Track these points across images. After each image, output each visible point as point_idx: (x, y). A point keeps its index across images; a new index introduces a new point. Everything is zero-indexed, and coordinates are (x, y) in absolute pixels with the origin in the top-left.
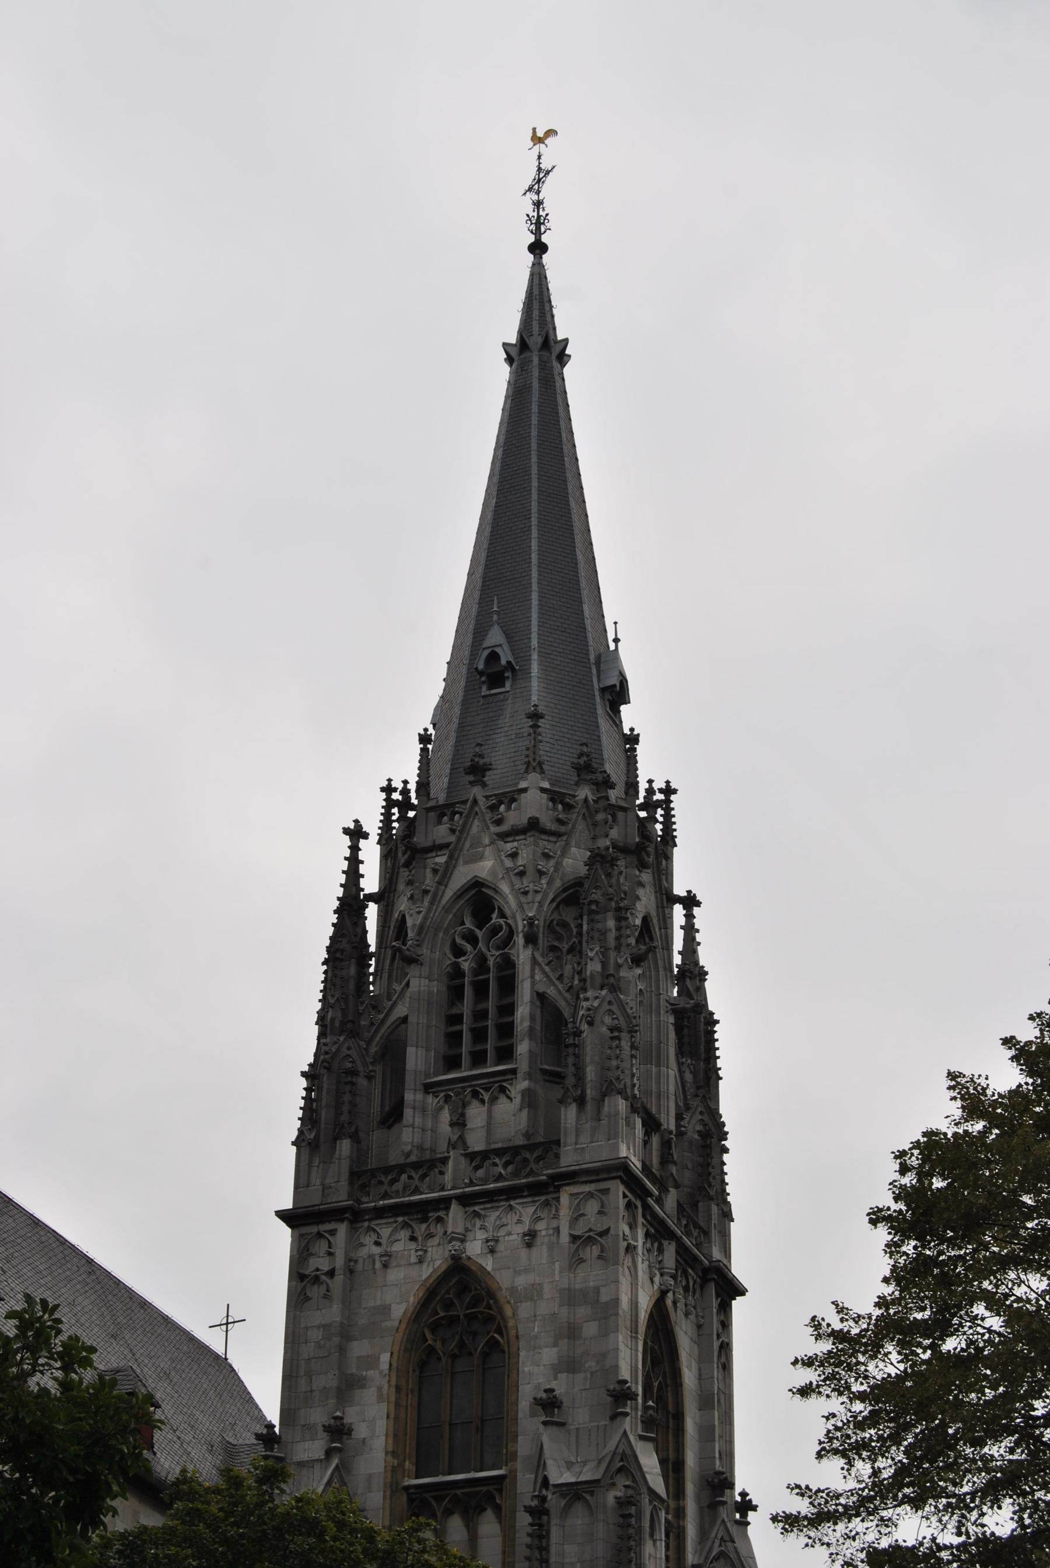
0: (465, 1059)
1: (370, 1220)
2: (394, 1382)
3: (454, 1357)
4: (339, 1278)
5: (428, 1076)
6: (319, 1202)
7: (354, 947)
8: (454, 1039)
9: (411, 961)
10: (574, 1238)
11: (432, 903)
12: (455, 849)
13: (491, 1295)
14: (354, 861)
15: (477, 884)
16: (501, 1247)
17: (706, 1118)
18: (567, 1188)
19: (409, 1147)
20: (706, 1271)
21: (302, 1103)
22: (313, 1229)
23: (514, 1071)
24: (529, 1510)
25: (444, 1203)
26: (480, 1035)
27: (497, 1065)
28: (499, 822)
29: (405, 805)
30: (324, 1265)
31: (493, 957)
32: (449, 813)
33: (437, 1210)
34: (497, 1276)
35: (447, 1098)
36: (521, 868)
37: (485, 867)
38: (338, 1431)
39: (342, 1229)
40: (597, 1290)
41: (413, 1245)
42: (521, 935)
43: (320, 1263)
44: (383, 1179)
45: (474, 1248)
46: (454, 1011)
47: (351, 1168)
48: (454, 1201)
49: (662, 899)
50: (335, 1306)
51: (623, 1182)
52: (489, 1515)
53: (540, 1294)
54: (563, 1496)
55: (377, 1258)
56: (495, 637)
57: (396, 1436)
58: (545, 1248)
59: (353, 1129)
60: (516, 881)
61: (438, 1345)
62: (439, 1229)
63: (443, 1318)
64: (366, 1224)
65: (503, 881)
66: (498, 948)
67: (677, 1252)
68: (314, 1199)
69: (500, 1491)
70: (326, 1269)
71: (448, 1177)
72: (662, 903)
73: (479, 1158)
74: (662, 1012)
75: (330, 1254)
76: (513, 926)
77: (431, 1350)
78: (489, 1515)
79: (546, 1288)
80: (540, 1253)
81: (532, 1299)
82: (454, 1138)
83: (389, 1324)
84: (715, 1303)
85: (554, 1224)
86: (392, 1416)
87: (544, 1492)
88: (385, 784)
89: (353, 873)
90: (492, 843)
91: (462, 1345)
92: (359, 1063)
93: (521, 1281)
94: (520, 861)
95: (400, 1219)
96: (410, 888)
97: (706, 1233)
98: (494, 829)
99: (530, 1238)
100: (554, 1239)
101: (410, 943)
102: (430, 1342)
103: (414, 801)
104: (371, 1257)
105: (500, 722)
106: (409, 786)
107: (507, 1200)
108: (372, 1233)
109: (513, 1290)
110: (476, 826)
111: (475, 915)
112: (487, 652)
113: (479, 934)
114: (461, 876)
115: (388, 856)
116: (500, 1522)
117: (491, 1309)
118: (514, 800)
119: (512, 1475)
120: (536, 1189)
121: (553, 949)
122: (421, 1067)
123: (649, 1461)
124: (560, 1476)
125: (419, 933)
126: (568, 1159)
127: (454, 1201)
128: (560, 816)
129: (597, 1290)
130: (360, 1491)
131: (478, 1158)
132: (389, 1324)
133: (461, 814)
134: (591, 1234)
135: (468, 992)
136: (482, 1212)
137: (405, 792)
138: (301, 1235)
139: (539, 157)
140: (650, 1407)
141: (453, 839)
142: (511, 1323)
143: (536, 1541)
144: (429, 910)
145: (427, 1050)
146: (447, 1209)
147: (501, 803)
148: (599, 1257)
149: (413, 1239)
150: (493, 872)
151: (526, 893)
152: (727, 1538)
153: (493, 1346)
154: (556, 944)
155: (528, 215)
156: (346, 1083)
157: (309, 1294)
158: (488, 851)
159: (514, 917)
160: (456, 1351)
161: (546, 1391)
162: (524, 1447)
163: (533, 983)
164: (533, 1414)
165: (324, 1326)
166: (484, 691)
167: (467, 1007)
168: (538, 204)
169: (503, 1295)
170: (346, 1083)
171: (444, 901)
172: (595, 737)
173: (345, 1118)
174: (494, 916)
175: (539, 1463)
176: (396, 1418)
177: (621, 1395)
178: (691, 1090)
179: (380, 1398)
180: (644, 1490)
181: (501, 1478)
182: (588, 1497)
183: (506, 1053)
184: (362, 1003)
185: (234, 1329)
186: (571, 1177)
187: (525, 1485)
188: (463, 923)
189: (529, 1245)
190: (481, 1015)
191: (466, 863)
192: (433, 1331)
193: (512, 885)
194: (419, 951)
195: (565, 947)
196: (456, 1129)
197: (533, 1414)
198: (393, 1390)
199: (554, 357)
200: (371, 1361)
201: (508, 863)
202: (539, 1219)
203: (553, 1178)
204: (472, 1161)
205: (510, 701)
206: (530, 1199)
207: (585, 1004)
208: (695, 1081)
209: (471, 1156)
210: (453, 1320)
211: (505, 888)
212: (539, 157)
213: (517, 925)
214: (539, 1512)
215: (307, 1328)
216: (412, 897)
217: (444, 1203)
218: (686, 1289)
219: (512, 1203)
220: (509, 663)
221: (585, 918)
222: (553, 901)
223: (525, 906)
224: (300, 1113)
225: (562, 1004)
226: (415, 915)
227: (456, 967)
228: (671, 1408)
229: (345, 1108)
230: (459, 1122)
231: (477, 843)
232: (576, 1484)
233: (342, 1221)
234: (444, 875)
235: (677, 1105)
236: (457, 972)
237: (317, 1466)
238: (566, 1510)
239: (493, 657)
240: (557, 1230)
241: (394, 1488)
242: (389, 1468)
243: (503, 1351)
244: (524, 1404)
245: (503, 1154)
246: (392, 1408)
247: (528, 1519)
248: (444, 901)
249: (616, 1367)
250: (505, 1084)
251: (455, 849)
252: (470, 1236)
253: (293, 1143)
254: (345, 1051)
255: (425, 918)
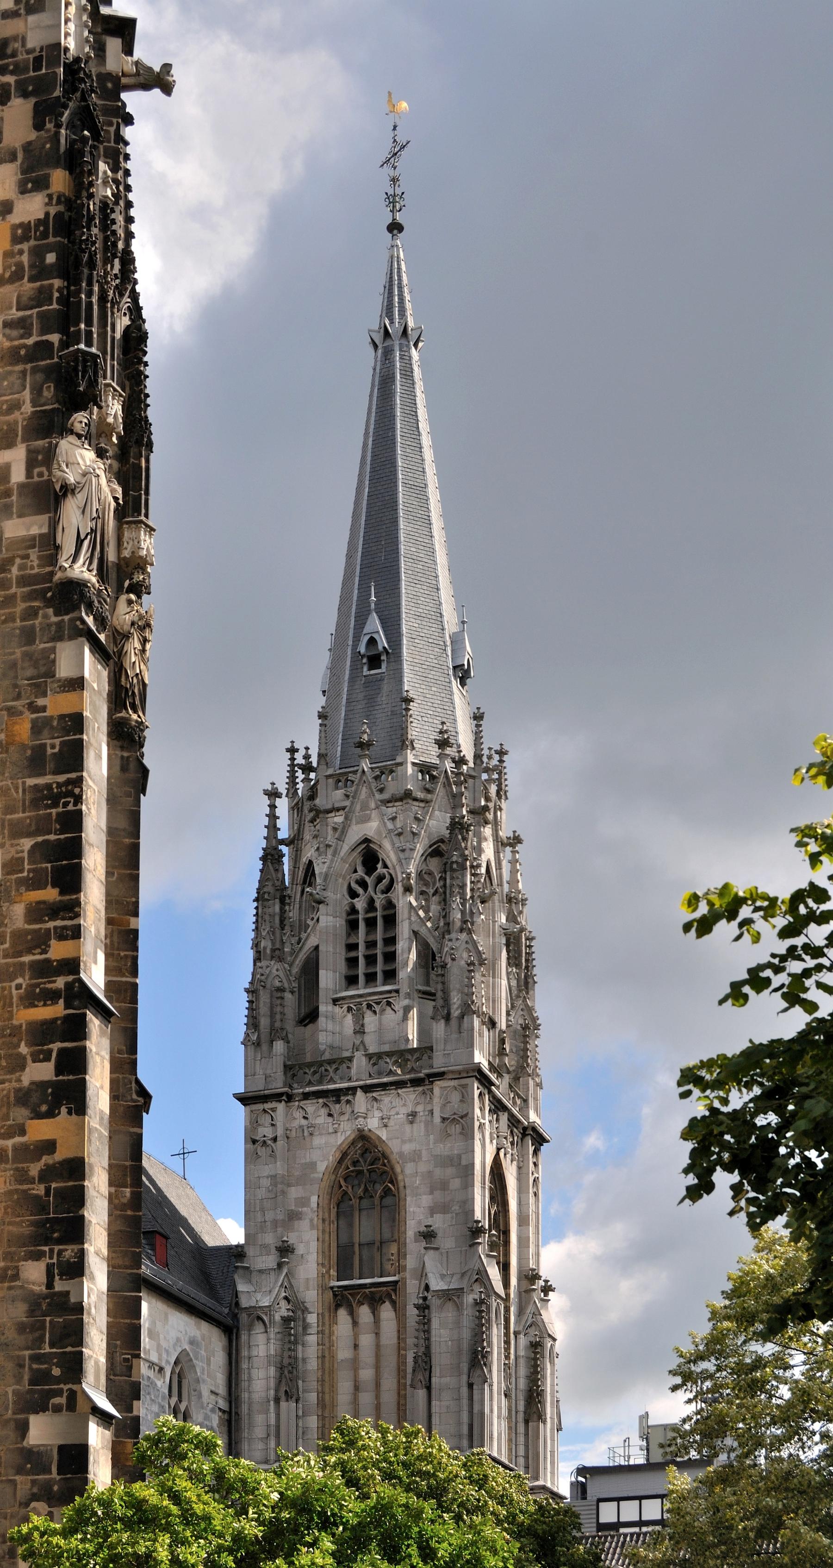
0: (362, 979)
1: (299, 1101)
2: (321, 1217)
3: (361, 1198)
4: (280, 1143)
5: (336, 992)
6: (261, 1088)
7: (277, 890)
8: (352, 962)
9: (320, 902)
10: (444, 1119)
11: (334, 854)
12: (349, 812)
13: (385, 1156)
14: (273, 817)
15: (367, 841)
16: (391, 1123)
17: (525, 1013)
18: (438, 1083)
19: (324, 1047)
20: (525, 1129)
21: (246, 1012)
22: (260, 1107)
23: (397, 991)
24: (417, 1307)
25: (353, 1090)
26: (371, 960)
27: (384, 985)
28: (381, 791)
29: (307, 768)
30: (268, 1132)
32: (343, 780)
33: (346, 1094)
34: (390, 1144)
35: (349, 1009)
36: (400, 830)
37: (372, 828)
38: (285, 1250)
39: (281, 1107)
40: (459, 1157)
41: (330, 1120)
42: (400, 884)
43: (266, 1131)
44: (307, 1071)
45: (373, 1124)
46: (352, 941)
47: (284, 1063)
48: (359, 1089)
49: (498, 846)
50: (278, 1163)
51: (477, 1078)
52: (387, 1306)
53: (420, 1157)
54: (439, 1298)
55: (305, 1128)
56: (374, 624)
57: (324, 1253)
58: (422, 1125)
59: (284, 1034)
60: (396, 839)
61: (350, 1191)
62: (348, 1109)
63: (352, 1171)
64: (297, 1103)
65: (386, 840)
66: (383, 892)
67: (509, 1120)
68: (259, 1086)
69: (395, 1291)
70: (271, 1136)
71: (354, 1071)
72: (498, 849)
73: (375, 1058)
74: (497, 935)
75: (273, 1125)
76: (394, 876)
77: (345, 1193)
78: (387, 1306)
79: (424, 1153)
80: (419, 1128)
81: (414, 1161)
82: (358, 1042)
83: (316, 1175)
84: (531, 1149)
85: (429, 1108)
86: (321, 1239)
87: (426, 1294)
88: (289, 746)
89: (272, 827)
90: (377, 807)
91: (366, 1190)
92: (284, 981)
94: (399, 824)
95: (321, 1100)
96: (315, 842)
97: (525, 1101)
98: (378, 796)
100: (429, 1118)
101: (318, 887)
102: (344, 1188)
103: (315, 764)
104: (301, 1127)
105: (379, 699)
106: (310, 752)
107: (396, 1089)
108: (301, 1110)
110: (364, 792)
111: (365, 863)
112: (367, 637)
114: (355, 834)
115: (296, 808)
116: (395, 1311)
117: (385, 1165)
118: (392, 771)
119: (404, 1280)
120: (416, 1082)
121: (422, 893)
122: (331, 986)
123: (494, 1273)
124: (436, 1284)
125: (325, 880)
126: (439, 1062)
127: (359, 1089)
128: (427, 786)
129: (459, 1157)
130: (301, 1290)
131: (375, 1058)
132: (316, 1175)
133: (353, 782)
134: (455, 1116)
135: (362, 925)
136: (378, 1097)
137: (307, 757)
138: (252, 1111)
139: (395, 128)
140: (494, 1235)
141: (347, 803)
142: (400, 1178)
143: (422, 1326)
144: (332, 861)
145: (335, 971)
146: (354, 1094)
147: (382, 773)
148: (461, 1133)
149: (330, 1115)
150: (378, 832)
151: (403, 851)
152: (537, 1313)
153: (387, 1192)
154: (424, 889)
155: (387, 194)
156: (277, 998)
157: (259, 1153)
158: (374, 814)
159: (394, 868)
160: (362, 1194)
161: (426, 1226)
162: (410, 1262)
163: (410, 924)
164: (416, 1241)
165: (271, 1176)
166: (365, 671)
167: (361, 936)
168: (394, 180)
169: (394, 1158)
170: (277, 998)
171: (342, 854)
172: (450, 713)
173: (278, 1024)
174: (379, 865)
175: (422, 1273)
176: (323, 1241)
177: (476, 1231)
178: (515, 992)
179: (312, 1227)
180: (492, 1293)
181: (396, 1282)
182: (455, 1298)
183: (390, 975)
184: (285, 934)
185: (189, 1158)
186: (441, 1075)
187: (412, 1287)
188: (355, 871)
189: (411, 1123)
190: (371, 945)
191: (357, 823)
192: (345, 1180)
193: (393, 844)
194: (325, 894)
195: (431, 891)
196: (358, 1036)
197: (416, 1241)
198: (321, 1221)
199: (412, 343)
200: (304, 1202)
201: (390, 825)
202: (418, 1103)
203: (429, 1076)
204: (370, 1059)
205: (386, 681)
206: (412, 1089)
207: (450, 944)
208: (518, 985)
209: (370, 1056)
210: (360, 1172)
211: (387, 845)
212: (395, 128)
213: (396, 875)
214: (424, 1308)
215: (259, 1177)
216: (318, 849)
217: (353, 1090)
218: (512, 1143)
219: (400, 1091)
220: (384, 648)
221: (448, 873)
222: (422, 855)
223: (403, 861)
224: (245, 1020)
225: (431, 941)
226: (321, 865)
228: (501, 1228)
229: (278, 1017)
230: (360, 1031)
231: (365, 807)
232: (448, 1290)
233: (280, 1101)
234: (341, 832)
235: (507, 1006)
236: (353, 910)
237: (272, 1273)
238: (441, 1307)
239: (372, 642)
240: (431, 1112)
241: (323, 1288)
242: (320, 1275)
243: (394, 1195)
244: (410, 1233)
245: (392, 1055)
246: (320, 1234)
247: (416, 1312)
248: (342, 854)
249: (473, 1211)
250: (390, 1000)
251: (349, 812)
252: (370, 1114)
253: (242, 1043)
254: (274, 971)
255: (329, 868)
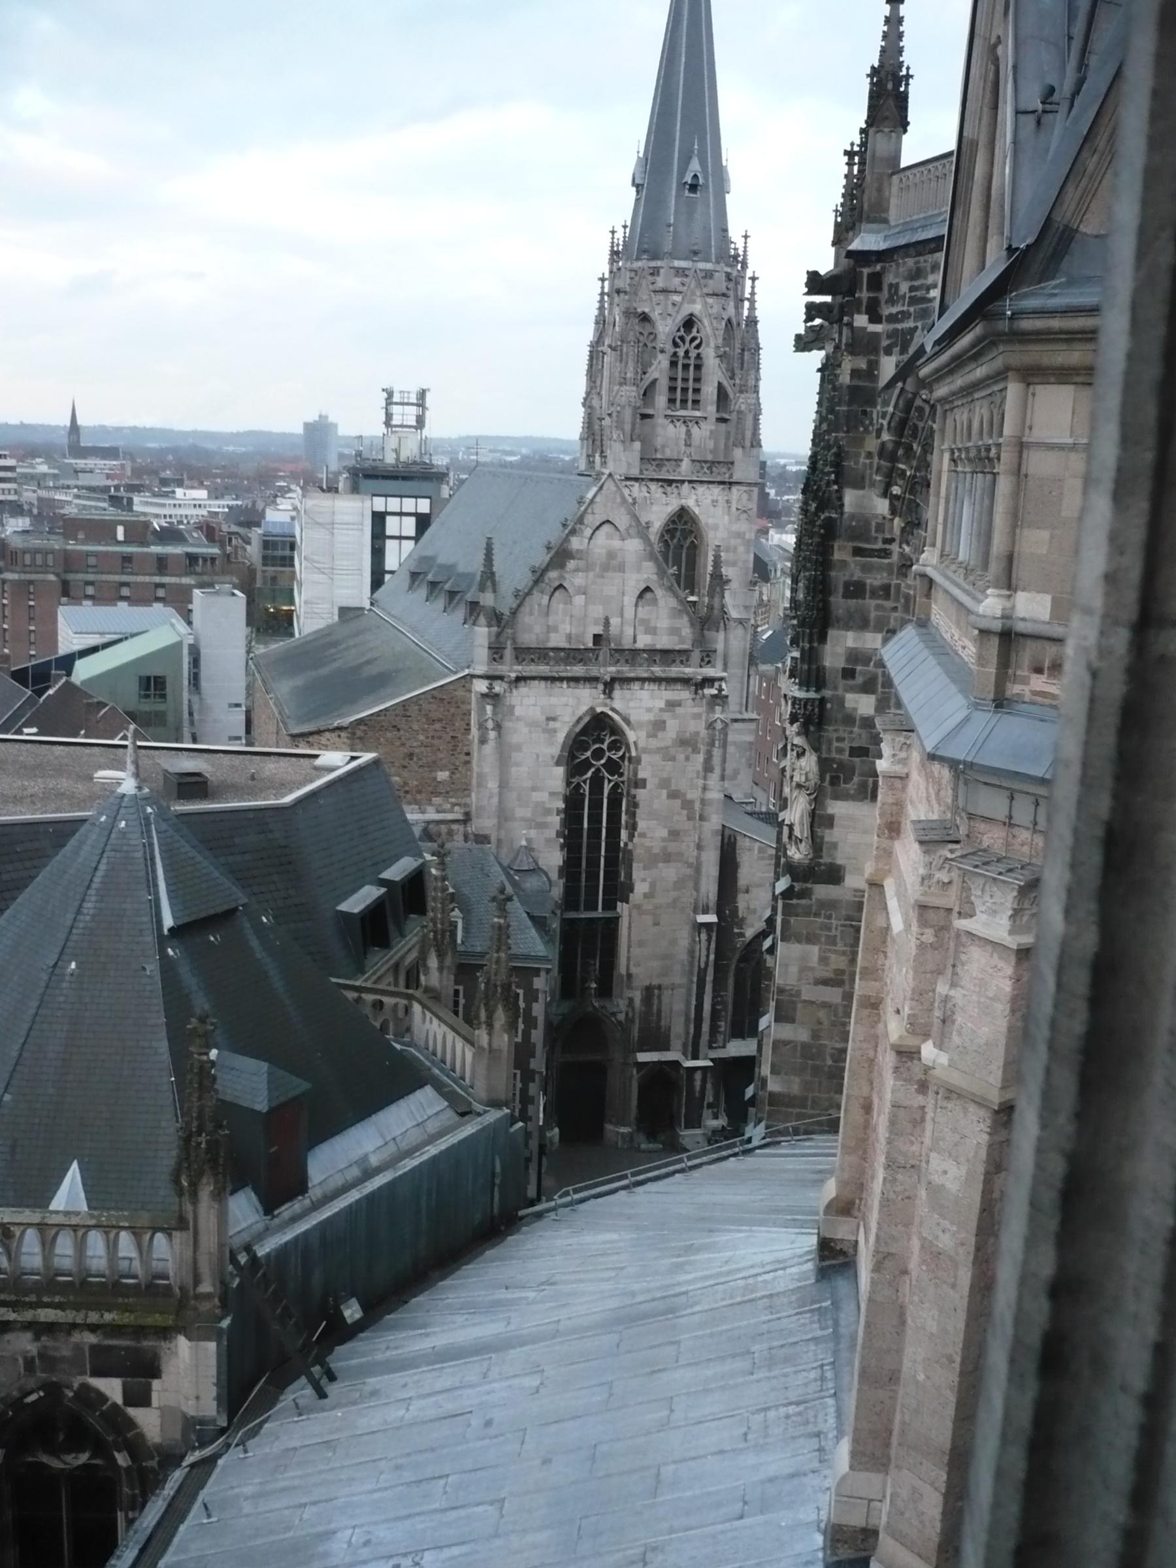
31: (693, 354)
34: (701, 517)
37: (697, 308)
45: (690, 503)
93: (711, 521)
99: (714, 503)
109: (707, 524)
113: (688, 339)
114: (686, 310)
158: (698, 300)
211: (706, 322)
227: (675, 354)
